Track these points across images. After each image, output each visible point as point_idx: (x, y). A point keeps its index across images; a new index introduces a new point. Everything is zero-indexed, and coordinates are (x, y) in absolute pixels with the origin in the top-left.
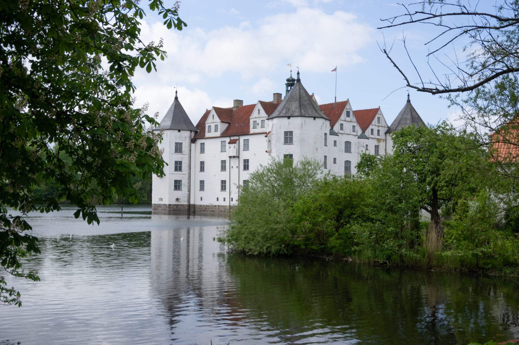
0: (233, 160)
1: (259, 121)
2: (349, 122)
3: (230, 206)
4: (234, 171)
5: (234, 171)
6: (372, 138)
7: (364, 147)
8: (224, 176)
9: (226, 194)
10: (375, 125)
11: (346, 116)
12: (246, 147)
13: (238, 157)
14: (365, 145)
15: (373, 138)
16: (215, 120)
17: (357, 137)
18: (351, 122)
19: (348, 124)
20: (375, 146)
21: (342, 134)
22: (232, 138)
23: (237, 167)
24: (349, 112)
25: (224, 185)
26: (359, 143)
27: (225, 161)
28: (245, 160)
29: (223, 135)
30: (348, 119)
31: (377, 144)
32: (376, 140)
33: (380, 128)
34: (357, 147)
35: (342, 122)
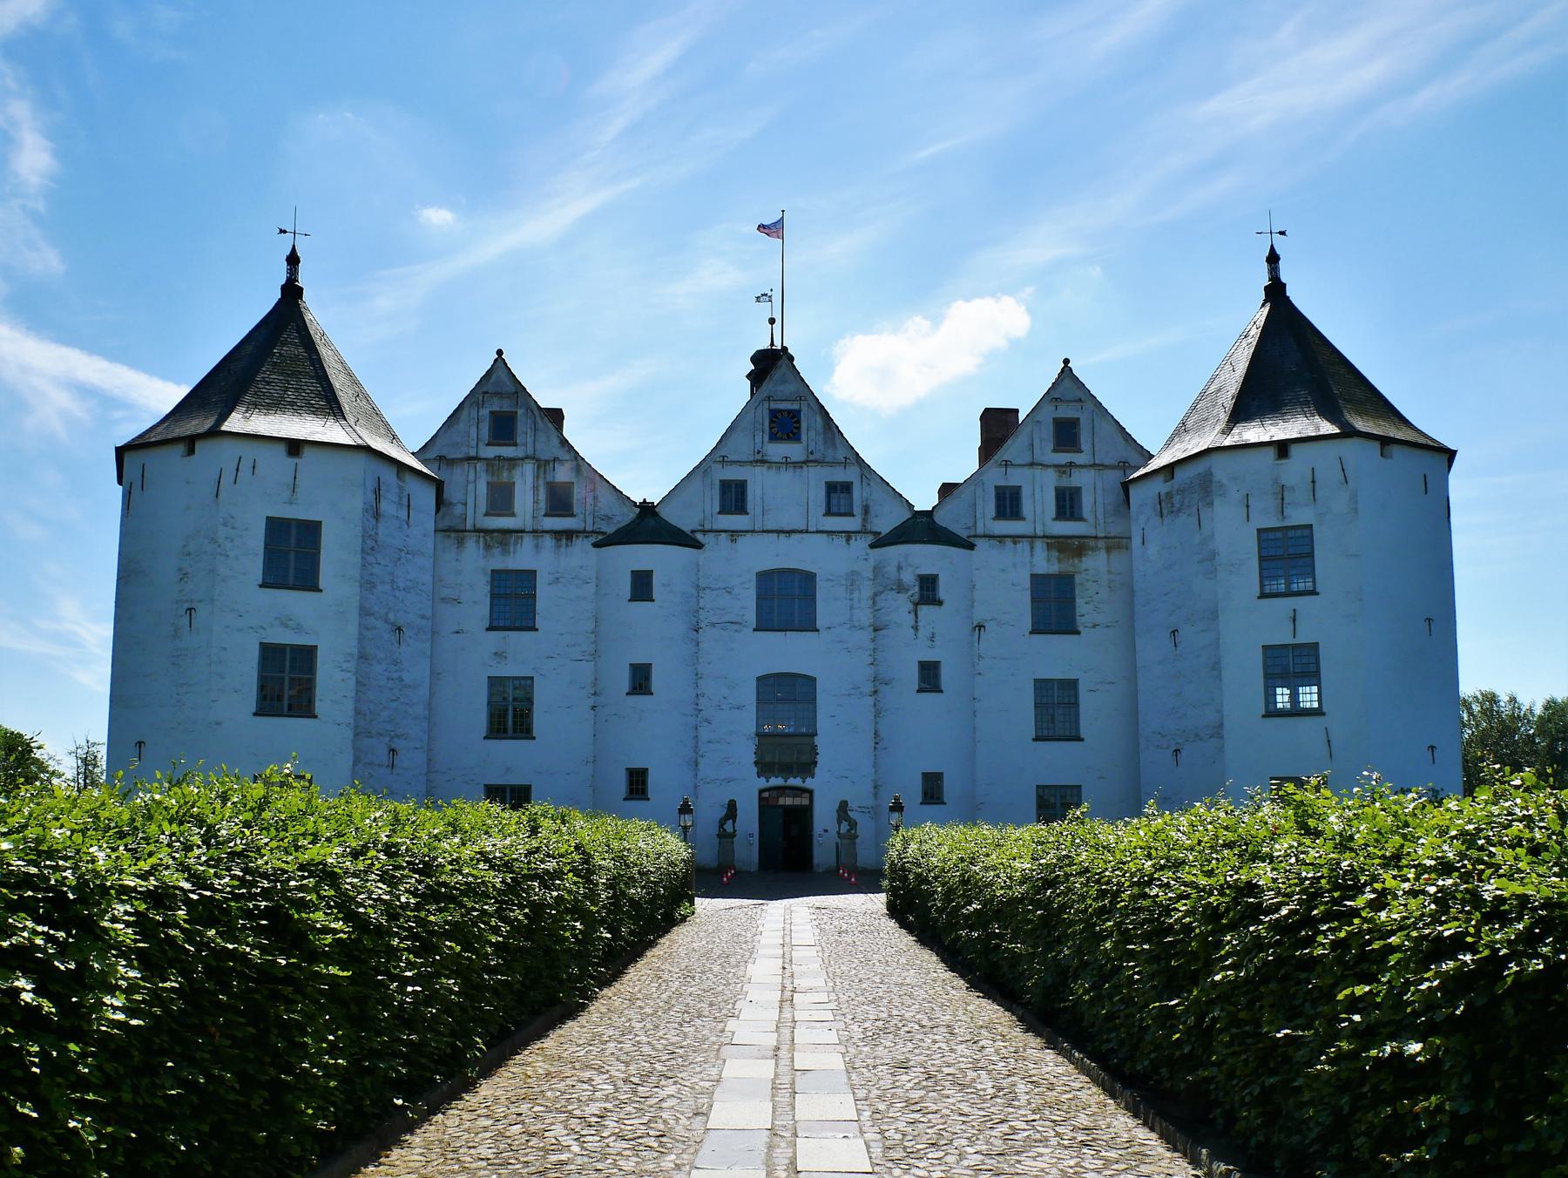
2: (798, 465)
6: (1001, 538)
7: (900, 588)
10: (1032, 464)
11: (762, 437)
14: (908, 577)
15: (1016, 538)
17: (870, 539)
18: (806, 462)
19: (787, 476)
20: (1039, 582)
21: (734, 534)
24: (795, 415)
26: (877, 569)
30: (778, 450)
31: (1054, 568)
32: (1039, 544)
33: (1079, 479)
34: (866, 591)
35: (733, 474)
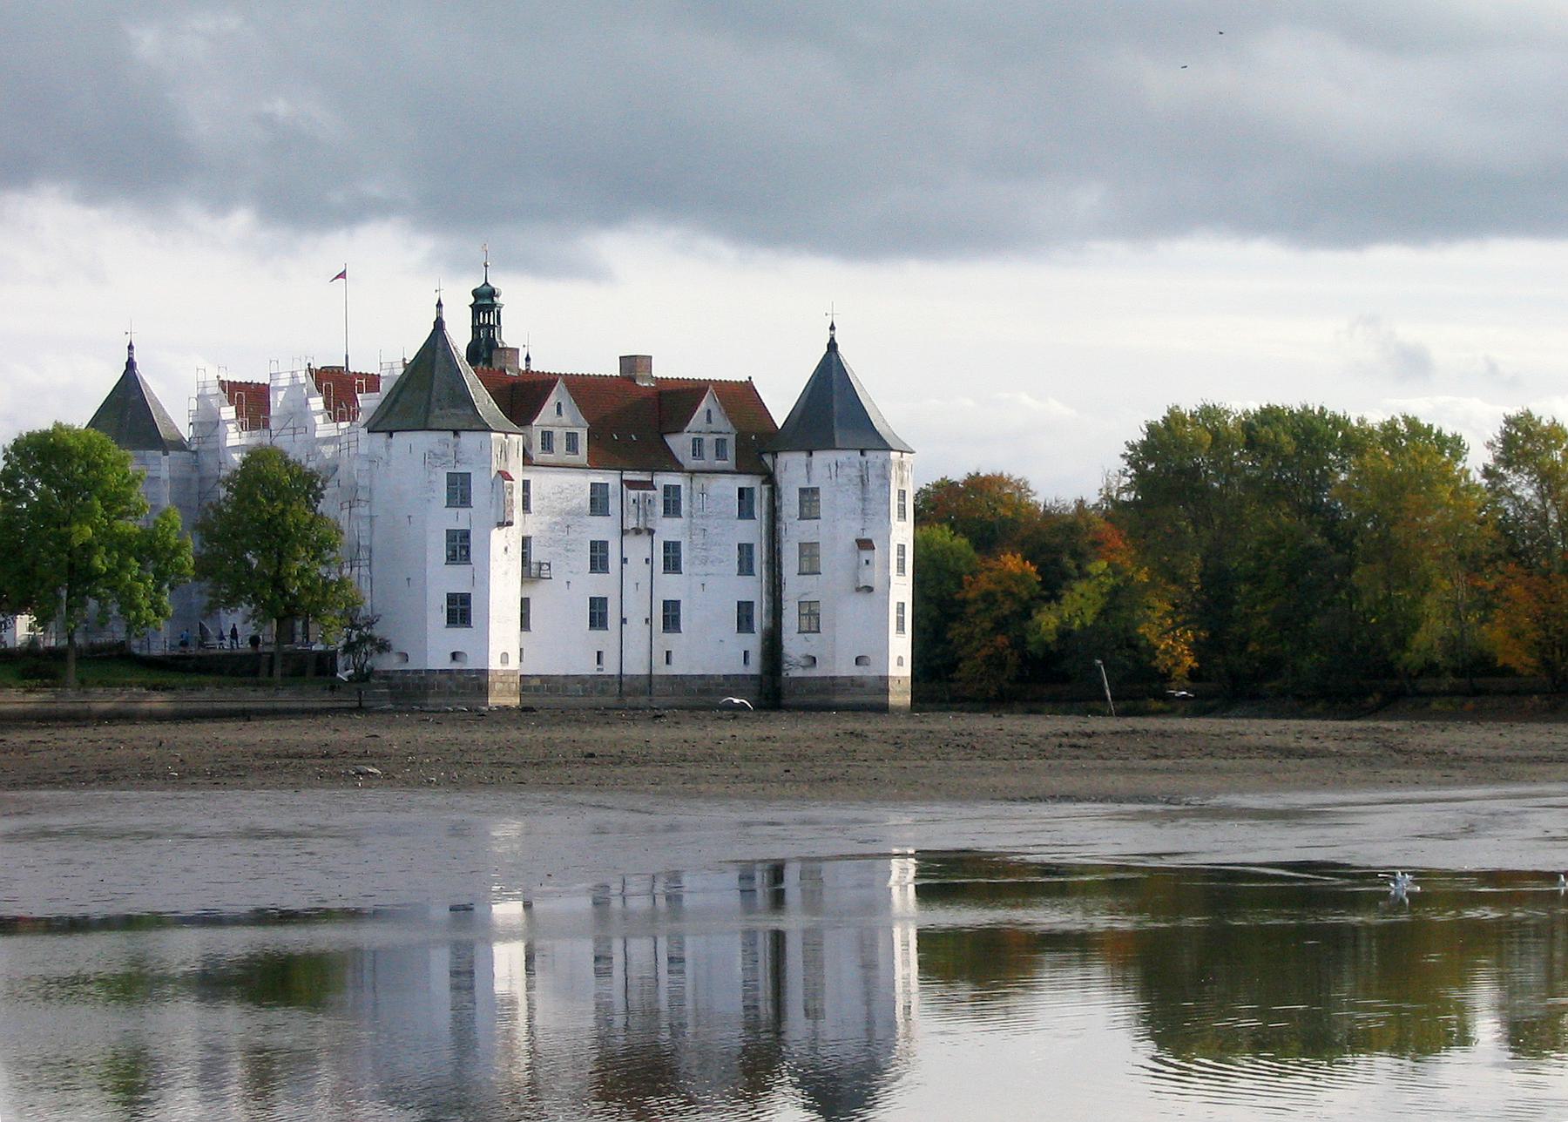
0: (630, 541)
1: (709, 440)
3: (621, 675)
4: (637, 569)
5: (637, 569)
8: (603, 585)
9: (606, 639)
12: (672, 506)
13: (651, 532)
16: (565, 418)
22: (629, 476)
23: (647, 560)
25: (459, 607)
27: (604, 544)
28: (666, 545)
29: (595, 463)
